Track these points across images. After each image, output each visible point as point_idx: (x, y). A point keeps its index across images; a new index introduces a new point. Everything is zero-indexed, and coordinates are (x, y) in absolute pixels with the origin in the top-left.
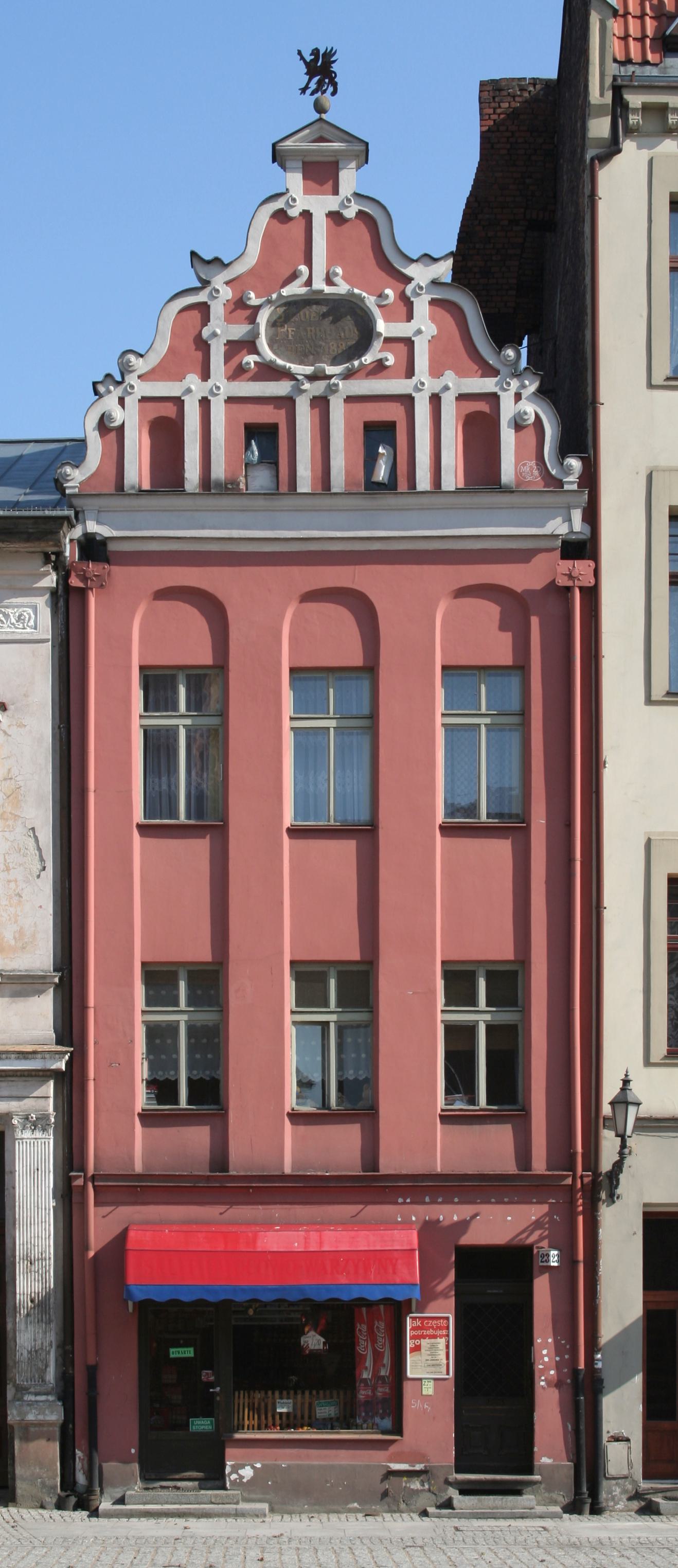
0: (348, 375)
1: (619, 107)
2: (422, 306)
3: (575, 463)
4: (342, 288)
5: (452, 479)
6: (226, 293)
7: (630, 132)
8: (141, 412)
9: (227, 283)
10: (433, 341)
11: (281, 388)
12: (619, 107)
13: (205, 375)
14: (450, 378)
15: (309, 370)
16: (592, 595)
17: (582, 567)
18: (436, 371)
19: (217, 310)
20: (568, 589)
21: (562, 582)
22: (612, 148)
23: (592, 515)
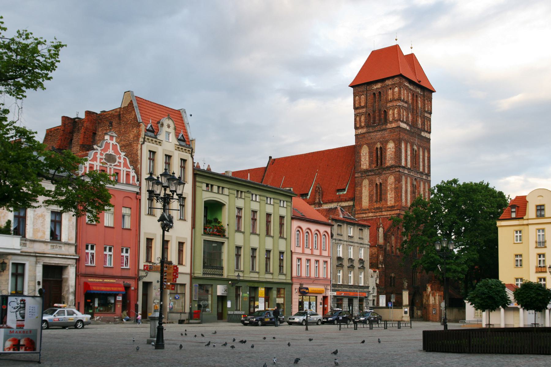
0: (115, 166)
1: (144, 138)
2: (122, 159)
3: (138, 182)
4: (114, 154)
5: (125, 182)
6: (100, 151)
7: (146, 141)
8: (89, 165)
9: (101, 150)
10: (124, 163)
11: (106, 166)
12: (144, 138)
13: (97, 162)
14: (125, 168)
15: (110, 164)
16: (140, 200)
17: (140, 196)
18: (124, 167)
19: (99, 153)
20: (137, 199)
21: (137, 198)
22: (144, 143)
23: (140, 189)
